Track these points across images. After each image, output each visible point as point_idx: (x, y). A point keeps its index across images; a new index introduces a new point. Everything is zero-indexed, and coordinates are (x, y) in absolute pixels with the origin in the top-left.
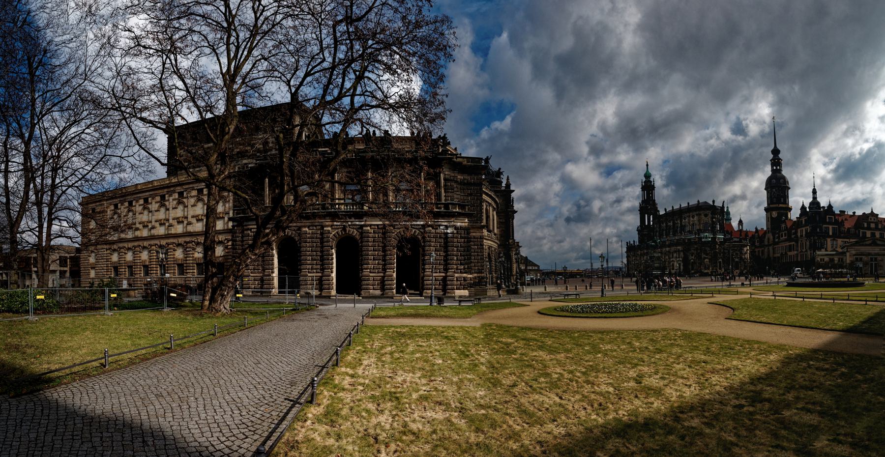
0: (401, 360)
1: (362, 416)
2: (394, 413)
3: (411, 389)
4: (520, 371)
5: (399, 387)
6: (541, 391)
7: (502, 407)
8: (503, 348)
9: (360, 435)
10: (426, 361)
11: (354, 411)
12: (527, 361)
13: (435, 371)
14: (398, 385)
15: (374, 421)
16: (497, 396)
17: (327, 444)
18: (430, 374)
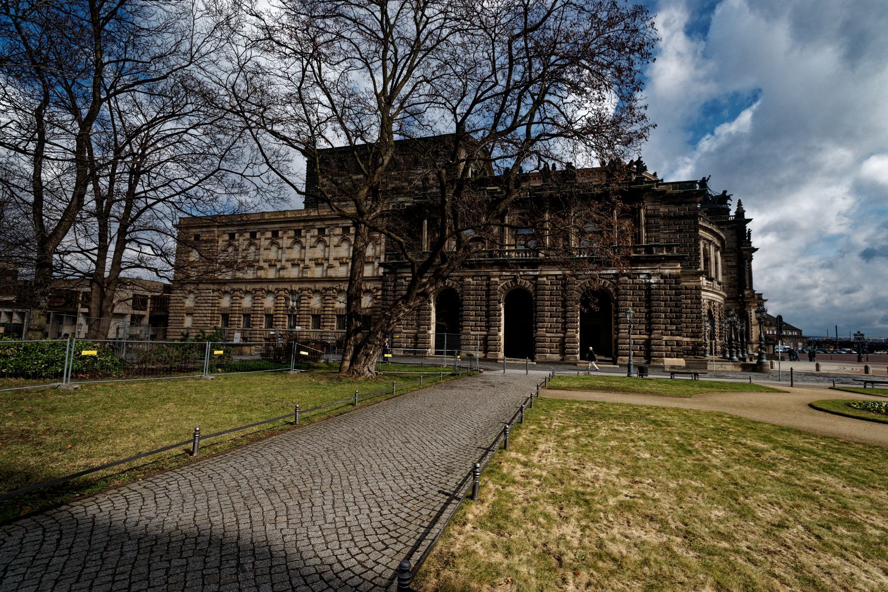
0: (591, 448)
1: (539, 523)
2: (583, 523)
3: (606, 490)
4: (791, 503)
5: (588, 486)
6: (844, 552)
7: (761, 558)
8: (748, 455)
9: (537, 551)
10: (626, 453)
11: (529, 514)
12: (803, 487)
13: (639, 468)
14: (587, 483)
15: (556, 532)
16: (750, 536)
17: (493, 560)
18: (633, 472)
